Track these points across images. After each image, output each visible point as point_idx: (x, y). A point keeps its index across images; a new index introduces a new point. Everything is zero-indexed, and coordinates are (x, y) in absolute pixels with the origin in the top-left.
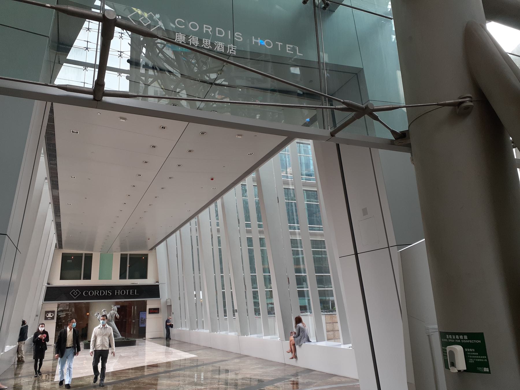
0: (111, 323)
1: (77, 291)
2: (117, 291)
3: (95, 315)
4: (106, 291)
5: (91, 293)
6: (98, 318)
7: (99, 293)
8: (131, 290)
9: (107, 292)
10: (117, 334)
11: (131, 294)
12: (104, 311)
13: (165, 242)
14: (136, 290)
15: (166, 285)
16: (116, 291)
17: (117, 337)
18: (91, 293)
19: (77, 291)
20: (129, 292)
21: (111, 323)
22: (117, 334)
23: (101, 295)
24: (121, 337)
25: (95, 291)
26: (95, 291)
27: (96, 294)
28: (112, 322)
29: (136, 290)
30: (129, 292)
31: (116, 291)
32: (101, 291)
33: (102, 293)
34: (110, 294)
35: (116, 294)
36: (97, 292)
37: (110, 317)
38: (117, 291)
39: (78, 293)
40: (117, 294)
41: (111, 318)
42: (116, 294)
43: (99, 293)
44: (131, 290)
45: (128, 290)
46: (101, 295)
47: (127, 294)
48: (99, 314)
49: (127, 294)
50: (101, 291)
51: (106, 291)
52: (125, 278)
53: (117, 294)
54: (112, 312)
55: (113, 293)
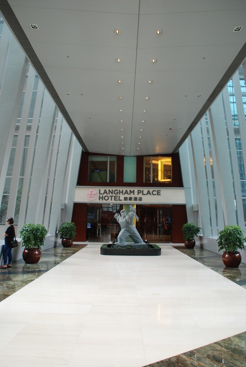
0: (130, 226)
12: (122, 212)
13: (189, 137)
15: (192, 189)
17: (138, 243)
21: (130, 226)
22: (138, 239)
24: (143, 243)
28: (131, 225)
37: (129, 219)
41: (130, 220)
54: (130, 213)
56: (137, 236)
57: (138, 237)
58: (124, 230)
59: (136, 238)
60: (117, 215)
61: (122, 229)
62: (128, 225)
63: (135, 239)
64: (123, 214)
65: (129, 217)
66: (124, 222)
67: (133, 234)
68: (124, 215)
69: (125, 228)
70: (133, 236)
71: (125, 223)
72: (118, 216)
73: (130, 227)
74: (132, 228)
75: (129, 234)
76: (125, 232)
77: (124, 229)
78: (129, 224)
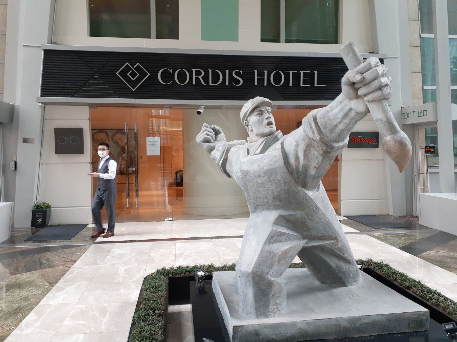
1: (138, 69)
2: (261, 74)
3: (200, 137)
4: (227, 71)
5: (182, 77)
6: (217, 154)
7: (206, 78)
8: (302, 72)
9: (230, 75)
10: (343, 265)
11: (301, 85)
14: (316, 72)
16: (256, 72)
18: (182, 77)
19: (138, 69)
20: (296, 77)
22: (343, 265)
23: (211, 84)
25: (194, 70)
26: (194, 70)
27: (197, 80)
29: (316, 72)
30: (296, 77)
31: (256, 72)
32: (210, 71)
33: (216, 77)
34: (239, 82)
35: (256, 84)
36: (198, 73)
38: (261, 74)
39: (143, 74)
40: (261, 81)
42: (256, 84)
43: (206, 78)
44: (302, 72)
45: (291, 72)
46: (211, 84)
47: (291, 85)
48: (217, 133)
49: (291, 85)
50: (210, 71)
51: (227, 71)
52: (276, 40)
53: (261, 81)
55: (249, 79)
56: (339, 249)
57: (346, 256)
58: (277, 222)
59: (333, 262)
60: (213, 134)
61: (254, 212)
62: (300, 189)
63: (329, 268)
64: (260, 122)
65: (317, 137)
66: (270, 173)
67: (322, 238)
68: (267, 130)
69: (276, 208)
70: (322, 248)
71: (282, 174)
72: (216, 140)
73: (311, 199)
74: (317, 207)
75: (301, 243)
76: (283, 234)
77: (273, 215)
78: (305, 186)
